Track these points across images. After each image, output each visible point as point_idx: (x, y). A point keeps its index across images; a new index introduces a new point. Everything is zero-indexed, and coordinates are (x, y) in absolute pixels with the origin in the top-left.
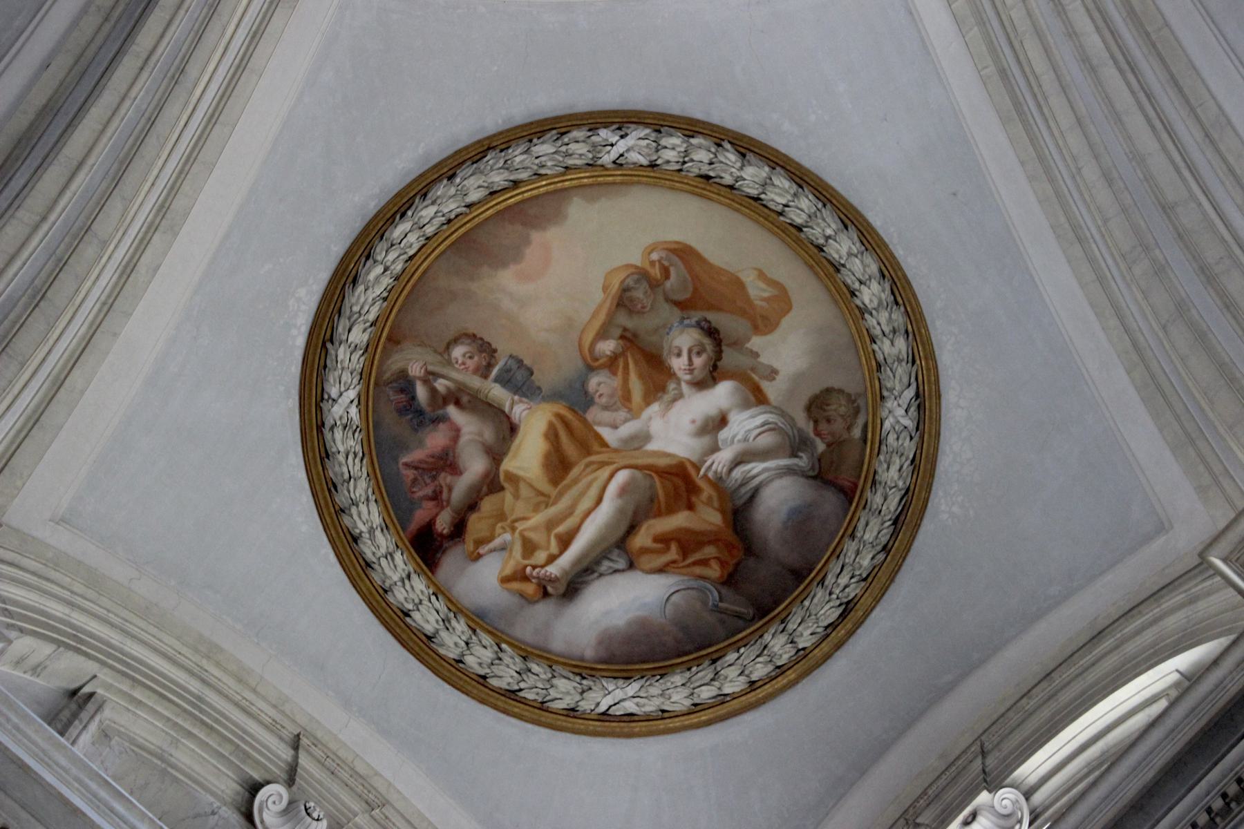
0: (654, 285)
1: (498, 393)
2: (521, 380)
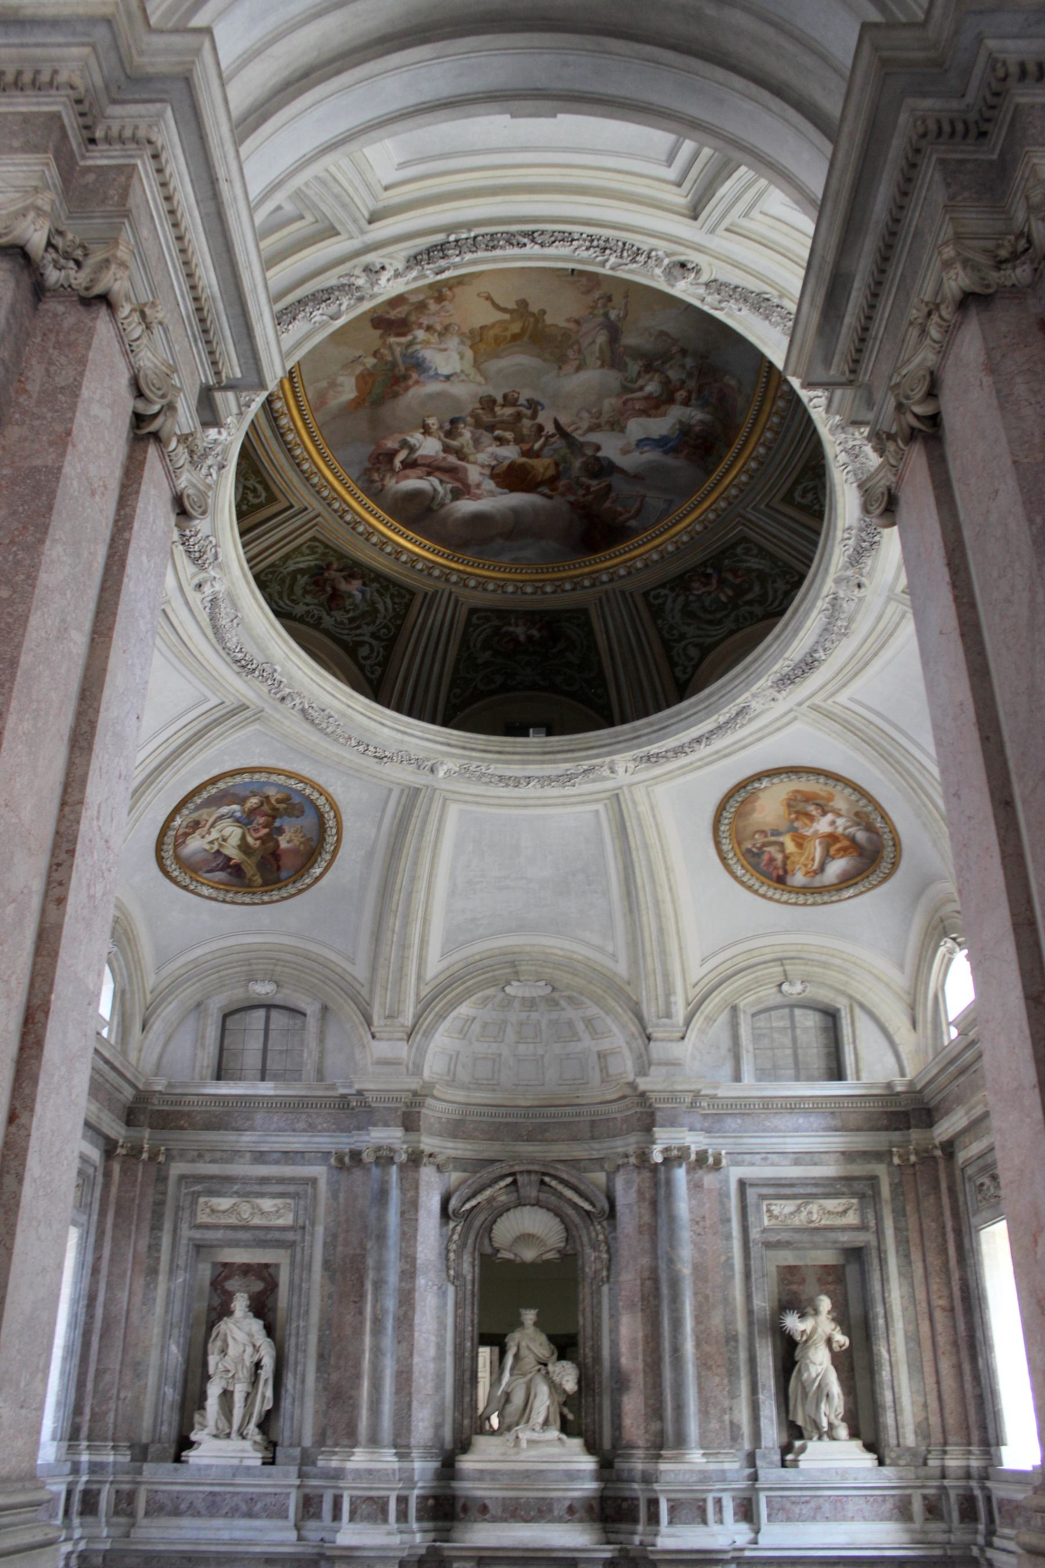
0: (795, 800)
1: (773, 839)
2: (776, 833)
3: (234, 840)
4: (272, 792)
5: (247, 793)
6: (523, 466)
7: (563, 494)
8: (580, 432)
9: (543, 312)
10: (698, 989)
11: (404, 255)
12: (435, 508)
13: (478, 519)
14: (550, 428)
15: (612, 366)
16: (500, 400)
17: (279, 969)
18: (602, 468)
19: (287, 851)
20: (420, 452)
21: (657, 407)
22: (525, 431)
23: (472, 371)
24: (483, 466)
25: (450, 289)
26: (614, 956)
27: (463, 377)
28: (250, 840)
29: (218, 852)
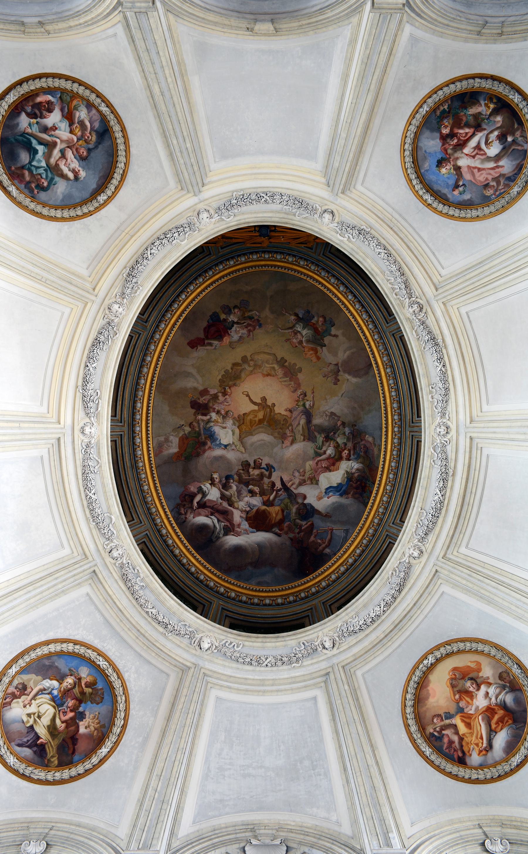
3: (46, 720)
4: (84, 673)
5: (68, 672)
6: (264, 511)
7: (287, 533)
8: (294, 486)
9: (274, 405)
10: (412, 840)
11: (215, 205)
12: (214, 539)
13: (238, 550)
14: (278, 485)
15: (309, 440)
16: (252, 464)
17: (52, 832)
18: (308, 512)
19: (84, 735)
20: (208, 497)
21: (333, 464)
22: (266, 487)
23: (238, 443)
24: (242, 511)
25: (230, 388)
26: (338, 823)
27: (233, 447)
28: (58, 722)
29: (32, 727)
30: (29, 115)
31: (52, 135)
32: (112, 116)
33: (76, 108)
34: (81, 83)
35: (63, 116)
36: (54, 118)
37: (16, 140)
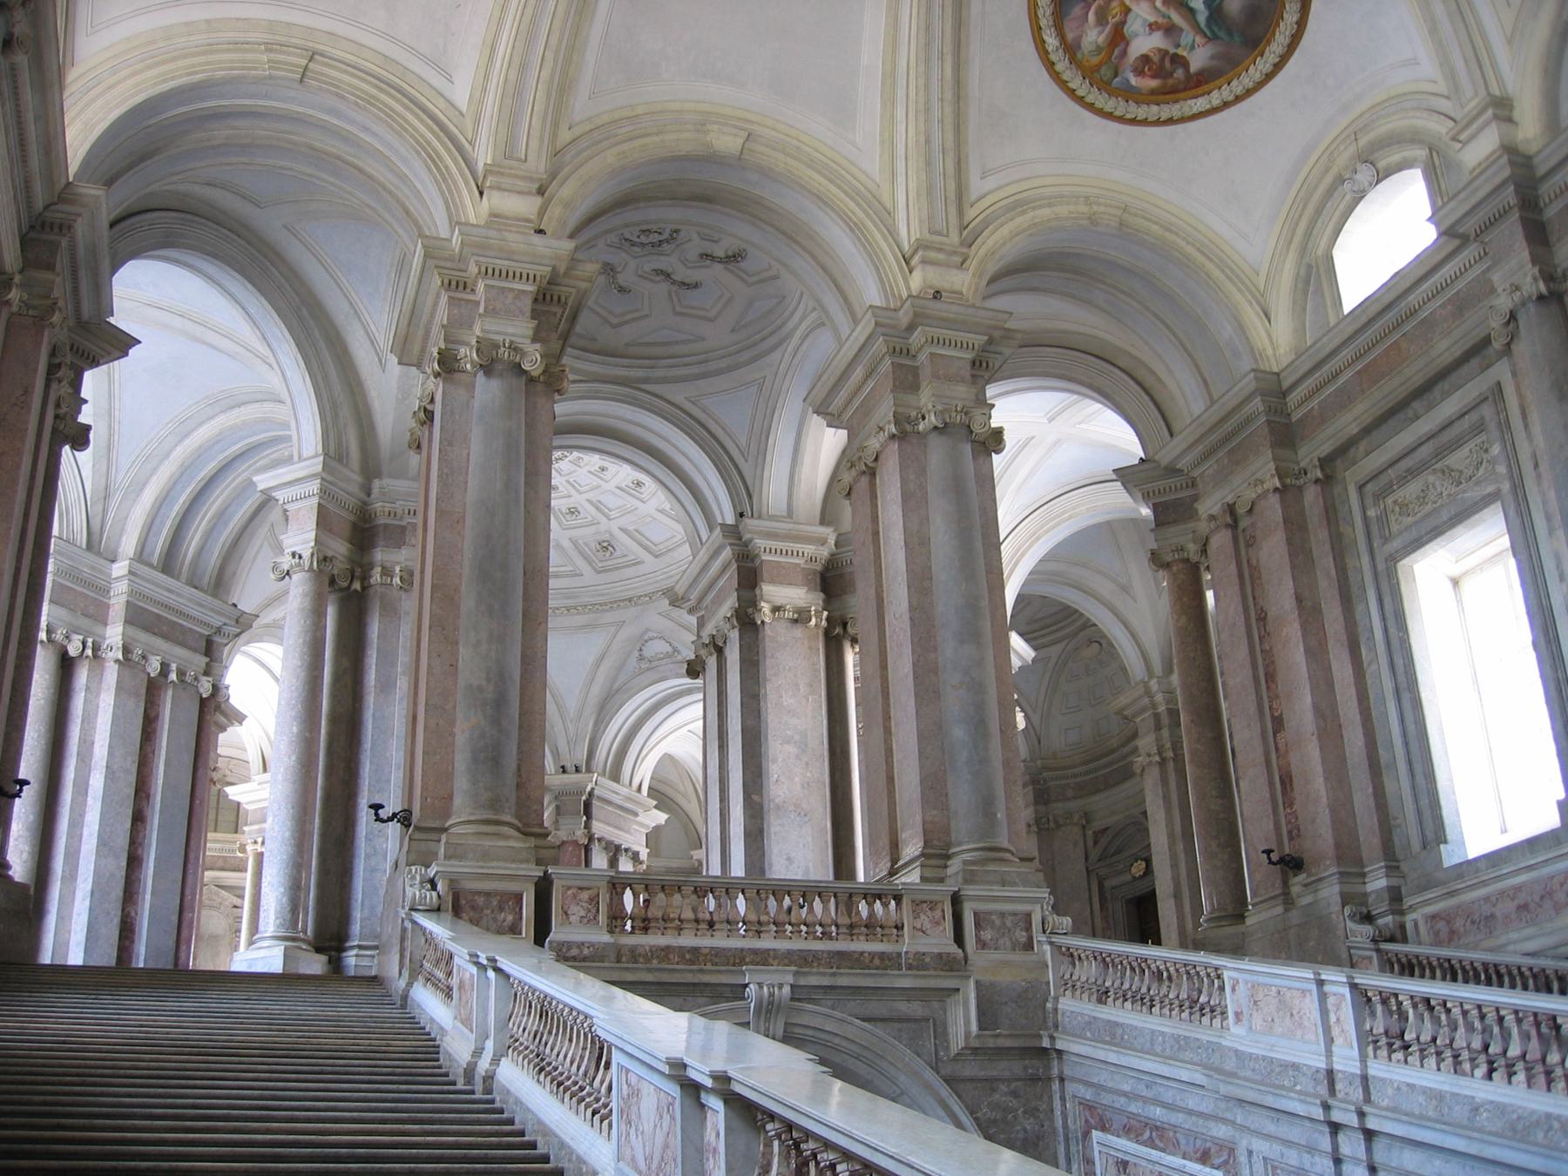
30: (1184, 63)
31: (1164, 16)
32: (1043, 23)
33: (1099, 49)
34: (1071, 93)
35: (1128, 44)
36: (1144, 43)
37: (1230, 34)
